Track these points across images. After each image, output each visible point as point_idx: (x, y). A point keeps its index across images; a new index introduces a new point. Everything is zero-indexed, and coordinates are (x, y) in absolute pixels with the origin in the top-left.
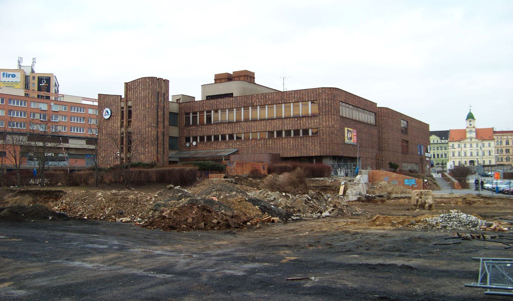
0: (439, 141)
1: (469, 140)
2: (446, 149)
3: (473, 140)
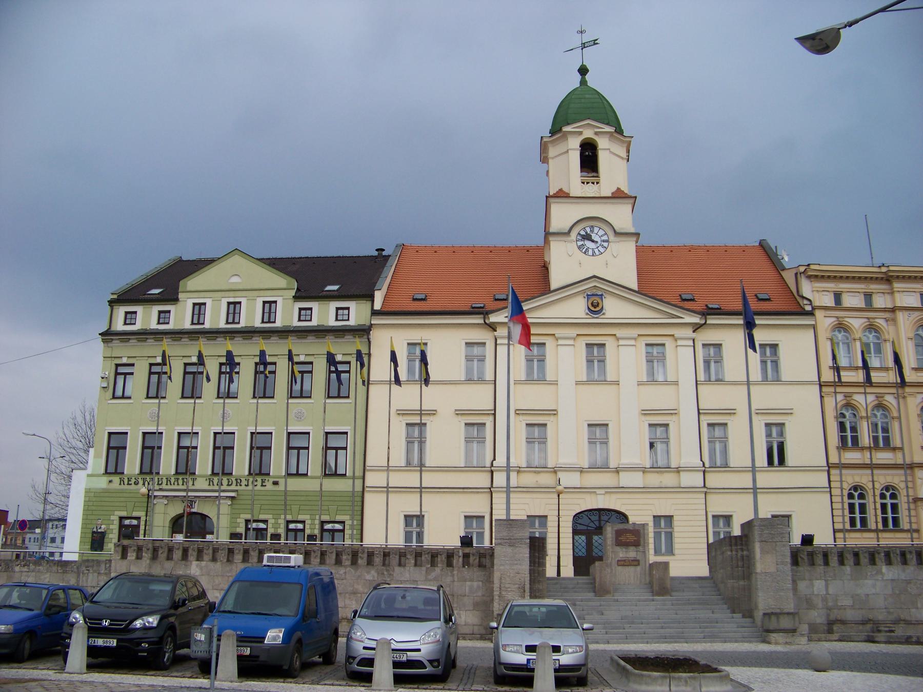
0: (287, 314)
1: (577, 308)
2: (337, 388)
3: (614, 309)
